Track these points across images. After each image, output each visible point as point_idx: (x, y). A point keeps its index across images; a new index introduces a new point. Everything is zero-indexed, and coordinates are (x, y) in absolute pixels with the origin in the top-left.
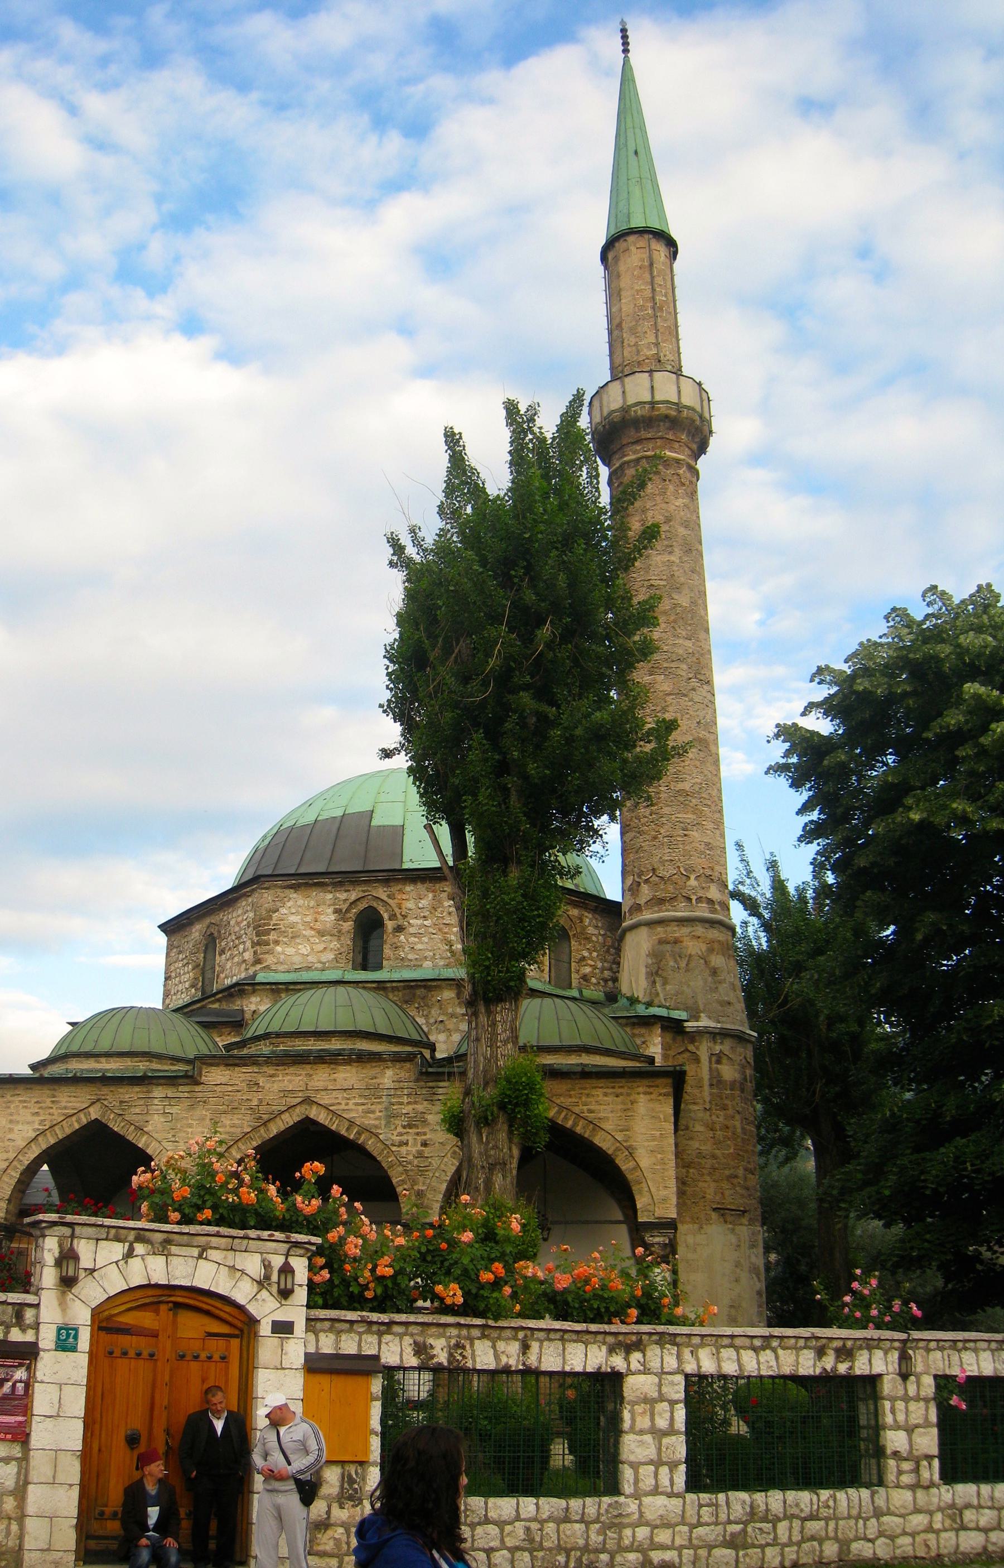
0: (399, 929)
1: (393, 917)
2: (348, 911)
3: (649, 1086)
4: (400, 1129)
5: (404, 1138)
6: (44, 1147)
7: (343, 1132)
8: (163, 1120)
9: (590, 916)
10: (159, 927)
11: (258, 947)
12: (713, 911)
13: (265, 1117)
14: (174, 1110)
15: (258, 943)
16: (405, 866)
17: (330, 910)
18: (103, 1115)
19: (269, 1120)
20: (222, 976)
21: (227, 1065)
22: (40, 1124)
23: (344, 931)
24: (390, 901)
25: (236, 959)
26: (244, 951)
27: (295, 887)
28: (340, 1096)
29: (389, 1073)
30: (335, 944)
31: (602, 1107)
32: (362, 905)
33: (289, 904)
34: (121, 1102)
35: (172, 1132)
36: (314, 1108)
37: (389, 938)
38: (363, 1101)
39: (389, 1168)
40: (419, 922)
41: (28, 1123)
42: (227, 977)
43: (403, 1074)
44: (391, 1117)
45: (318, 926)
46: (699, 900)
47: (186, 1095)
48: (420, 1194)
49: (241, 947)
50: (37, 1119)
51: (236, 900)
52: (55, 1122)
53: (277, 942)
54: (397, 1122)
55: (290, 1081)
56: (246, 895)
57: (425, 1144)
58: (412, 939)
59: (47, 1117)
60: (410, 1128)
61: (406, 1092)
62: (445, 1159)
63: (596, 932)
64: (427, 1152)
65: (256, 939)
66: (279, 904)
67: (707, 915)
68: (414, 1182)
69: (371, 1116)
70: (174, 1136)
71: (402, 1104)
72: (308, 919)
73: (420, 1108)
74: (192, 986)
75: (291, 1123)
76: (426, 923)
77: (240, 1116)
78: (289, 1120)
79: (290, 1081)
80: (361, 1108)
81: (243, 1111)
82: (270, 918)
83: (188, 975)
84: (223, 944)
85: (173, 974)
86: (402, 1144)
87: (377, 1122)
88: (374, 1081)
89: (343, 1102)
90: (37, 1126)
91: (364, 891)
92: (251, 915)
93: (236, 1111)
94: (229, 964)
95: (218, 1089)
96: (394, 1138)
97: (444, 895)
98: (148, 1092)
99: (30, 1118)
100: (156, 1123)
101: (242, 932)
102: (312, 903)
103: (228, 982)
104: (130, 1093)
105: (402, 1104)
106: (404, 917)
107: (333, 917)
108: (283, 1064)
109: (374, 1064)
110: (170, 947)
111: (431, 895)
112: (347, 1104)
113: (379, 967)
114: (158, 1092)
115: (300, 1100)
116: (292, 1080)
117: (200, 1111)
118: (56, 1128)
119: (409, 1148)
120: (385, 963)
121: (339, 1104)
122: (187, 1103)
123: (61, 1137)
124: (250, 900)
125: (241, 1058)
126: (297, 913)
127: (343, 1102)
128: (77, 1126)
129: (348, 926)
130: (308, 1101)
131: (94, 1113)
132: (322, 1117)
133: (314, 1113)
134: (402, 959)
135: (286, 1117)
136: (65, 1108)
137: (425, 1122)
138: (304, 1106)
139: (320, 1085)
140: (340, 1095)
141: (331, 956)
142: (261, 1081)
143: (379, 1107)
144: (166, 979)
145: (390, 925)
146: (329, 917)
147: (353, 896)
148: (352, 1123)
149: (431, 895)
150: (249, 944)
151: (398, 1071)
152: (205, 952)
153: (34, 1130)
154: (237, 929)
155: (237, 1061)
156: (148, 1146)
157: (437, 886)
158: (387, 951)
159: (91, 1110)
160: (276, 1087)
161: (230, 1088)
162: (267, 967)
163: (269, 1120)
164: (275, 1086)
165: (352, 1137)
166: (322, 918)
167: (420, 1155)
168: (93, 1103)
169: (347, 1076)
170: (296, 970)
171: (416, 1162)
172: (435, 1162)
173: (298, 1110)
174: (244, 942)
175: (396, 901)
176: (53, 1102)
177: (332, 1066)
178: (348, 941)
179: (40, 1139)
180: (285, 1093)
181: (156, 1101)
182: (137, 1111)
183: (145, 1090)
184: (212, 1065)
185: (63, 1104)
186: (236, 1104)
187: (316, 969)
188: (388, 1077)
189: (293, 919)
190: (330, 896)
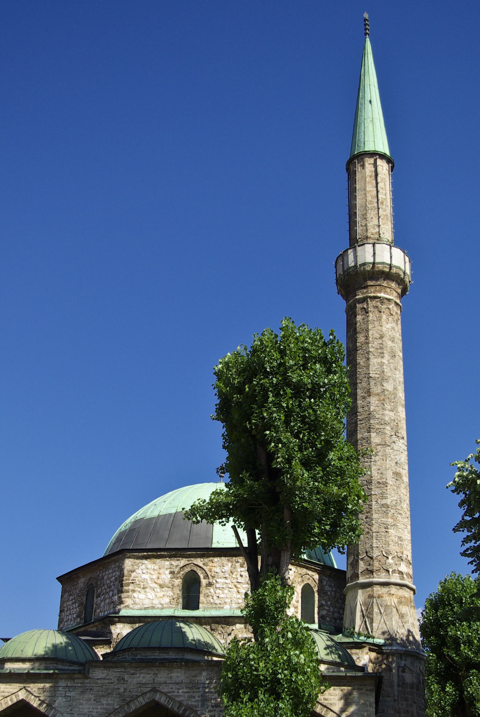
0: (210, 584)
1: (207, 576)
2: (178, 573)
3: (361, 685)
7: (176, 709)
8: (64, 700)
9: (327, 579)
10: (57, 578)
12: (402, 578)
13: (128, 699)
14: (72, 694)
16: (214, 546)
17: (168, 572)
18: (27, 697)
19: (130, 701)
20: (98, 611)
23: (175, 585)
24: (204, 567)
25: (107, 601)
26: (113, 595)
28: (174, 687)
29: (204, 674)
30: (170, 593)
31: (332, 697)
32: (187, 569)
35: (70, 708)
37: (203, 590)
38: (188, 690)
42: (101, 612)
45: (160, 582)
46: (394, 571)
49: (111, 593)
53: (134, 591)
55: (144, 678)
58: (218, 591)
63: (330, 589)
66: (135, 567)
67: (399, 581)
69: (193, 699)
74: (78, 616)
76: (227, 581)
77: (113, 699)
78: (142, 701)
79: (144, 678)
80: (186, 695)
83: (75, 609)
84: (99, 591)
85: (66, 609)
87: (196, 704)
88: (195, 678)
89: (176, 691)
94: (103, 604)
95: (99, 681)
97: (238, 565)
101: (112, 584)
102: (156, 567)
103: (102, 614)
106: (213, 577)
107: (169, 576)
110: (64, 592)
111: (230, 564)
112: (178, 692)
113: (197, 608)
115: (150, 689)
116: (144, 677)
120: (201, 605)
121: (173, 692)
125: (114, 662)
127: (176, 691)
128: (10, 703)
129: (178, 582)
130: (154, 690)
131: (22, 695)
132: (163, 700)
133: (157, 697)
134: (211, 603)
135: (140, 699)
136: (3, 692)
138: (152, 693)
139: (163, 680)
141: (167, 600)
142: (126, 677)
143: (198, 694)
144: (61, 612)
145: (204, 582)
146: (166, 576)
148: (181, 704)
149: (230, 564)
150: (116, 591)
152: (87, 595)
154: (108, 582)
155: (112, 665)
158: (202, 598)
159: (20, 693)
161: (107, 681)
162: (127, 606)
163: (130, 701)
168: (21, 689)
170: (145, 608)
173: (148, 695)
174: (113, 591)
175: (208, 567)
178: (178, 592)
180: (141, 685)
181: (60, 689)
184: (96, 667)
187: (158, 608)
189: (144, 576)
190: (167, 563)
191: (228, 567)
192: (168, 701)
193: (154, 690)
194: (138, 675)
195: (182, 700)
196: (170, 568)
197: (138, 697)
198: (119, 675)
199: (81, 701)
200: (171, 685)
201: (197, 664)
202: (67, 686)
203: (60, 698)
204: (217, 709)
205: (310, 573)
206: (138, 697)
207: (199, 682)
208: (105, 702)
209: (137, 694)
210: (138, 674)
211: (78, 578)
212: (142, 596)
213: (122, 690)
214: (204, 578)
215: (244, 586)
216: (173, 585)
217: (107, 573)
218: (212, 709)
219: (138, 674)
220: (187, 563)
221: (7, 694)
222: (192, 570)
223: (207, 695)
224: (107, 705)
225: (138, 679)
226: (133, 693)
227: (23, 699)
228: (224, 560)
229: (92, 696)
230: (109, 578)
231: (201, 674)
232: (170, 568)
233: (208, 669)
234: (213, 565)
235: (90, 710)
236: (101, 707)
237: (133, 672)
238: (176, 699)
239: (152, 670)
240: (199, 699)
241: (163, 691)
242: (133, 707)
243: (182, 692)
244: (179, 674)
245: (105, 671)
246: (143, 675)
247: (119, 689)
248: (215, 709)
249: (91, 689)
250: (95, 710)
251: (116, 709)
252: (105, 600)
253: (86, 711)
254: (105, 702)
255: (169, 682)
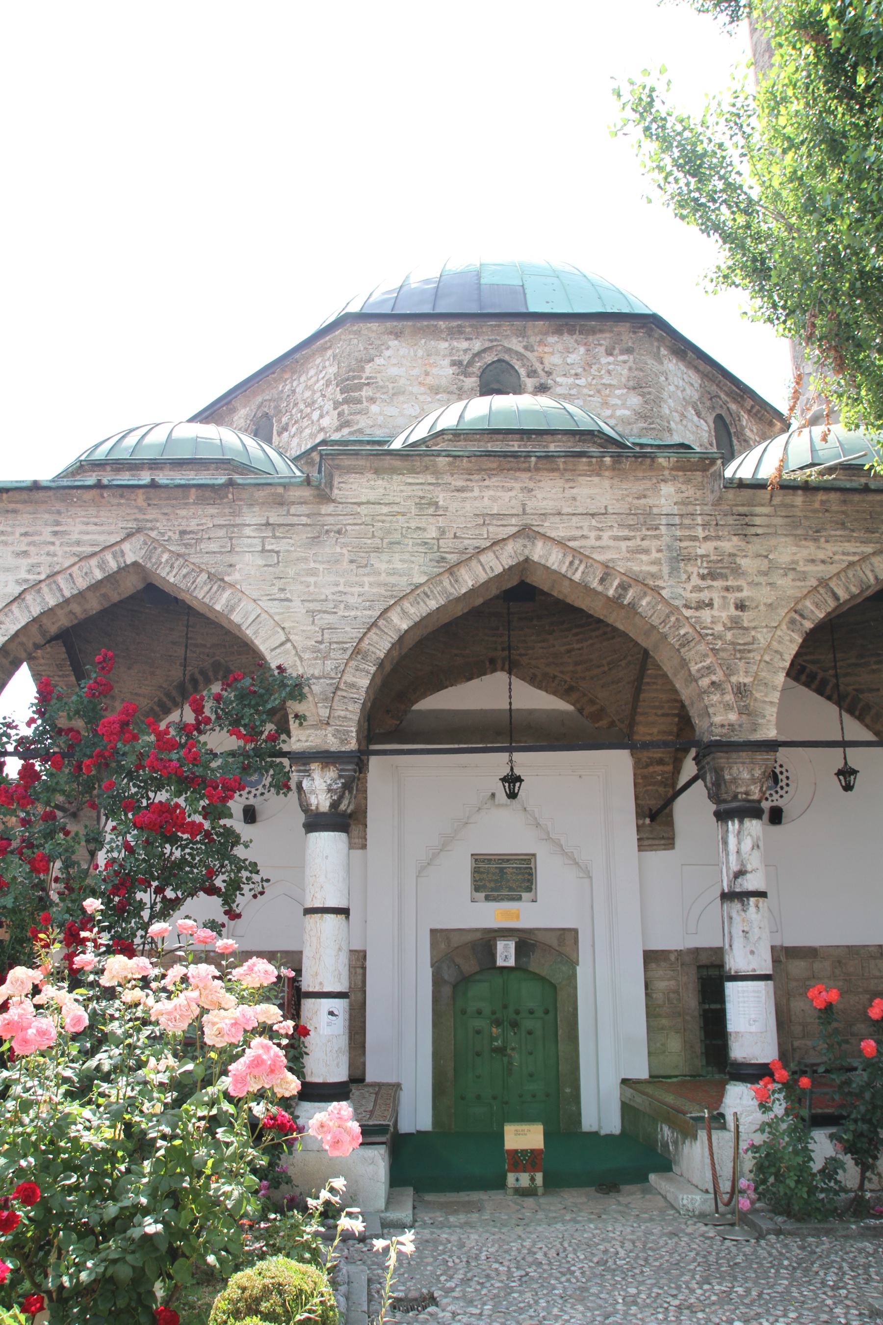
1: (532, 373)
2: (471, 363)
4: (695, 581)
5: (705, 596)
6: (36, 611)
7: (595, 584)
8: (261, 562)
11: (345, 407)
13: (453, 558)
14: (282, 545)
15: (346, 401)
17: (447, 362)
21: (377, 472)
22: (29, 571)
23: (466, 388)
24: (528, 354)
26: (321, 416)
27: (398, 335)
28: (586, 524)
29: (668, 489)
32: (489, 358)
33: (387, 353)
34: (183, 533)
35: (279, 584)
36: (539, 544)
38: (626, 533)
39: (683, 645)
40: (570, 380)
41: (8, 570)
43: (690, 492)
44: (680, 559)
45: (429, 380)
47: (304, 520)
48: (741, 691)
49: (315, 415)
50: (25, 562)
51: (307, 359)
52: (57, 568)
53: (372, 400)
54: (690, 569)
55: (493, 499)
56: (325, 349)
57: (741, 606)
59: (44, 559)
60: (713, 579)
61: (699, 520)
62: (779, 633)
64: (746, 618)
65: (340, 398)
68: (730, 671)
69: (644, 557)
70: (282, 590)
71: (694, 538)
72: (415, 372)
73: (728, 545)
75: (499, 570)
76: (577, 382)
77: (406, 556)
78: (494, 564)
79: (493, 499)
80: (624, 545)
81: (410, 548)
82: (362, 369)
84: (284, 420)
86: (701, 605)
87: (654, 569)
89: (593, 534)
90: (24, 575)
91: (491, 341)
92: (332, 370)
93: (397, 548)
95: (363, 510)
96: (688, 595)
98: (233, 514)
99: (11, 561)
100: (247, 567)
102: (420, 353)
104: (198, 517)
105: (694, 538)
106: (549, 374)
107: (450, 371)
108: (480, 470)
109: (640, 474)
111: (582, 350)
112: (599, 538)
114: (252, 517)
115: (514, 530)
116: (499, 497)
117: (330, 548)
118: (60, 579)
119: (715, 613)
122: (304, 535)
123: (67, 594)
124: (330, 353)
126: (400, 365)
127: (593, 534)
128: (99, 575)
130: (527, 533)
131: (132, 553)
132: (554, 559)
133: (538, 552)
135: (488, 558)
136: (78, 543)
137: (737, 571)
139: (548, 505)
140: (586, 523)
146: (444, 371)
147: (477, 346)
149: (582, 350)
150: (329, 406)
151: (684, 487)
153: (18, 582)
154: (308, 394)
155: (397, 463)
156: (232, 609)
157: (591, 338)
159: (126, 546)
160: (468, 508)
161: (385, 510)
164: (468, 506)
165: (611, 593)
166: (434, 371)
167: (735, 624)
168: (129, 536)
169: (597, 491)
171: (729, 636)
172: (762, 637)
175: (536, 354)
176: (55, 533)
177: (568, 475)
179: (29, 597)
180: (486, 518)
181: (248, 531)
182: (213, 546)
183: (227, 511)
184: (350, 470)
185: (75, 537)
186: (397, 536)
188: (667, 496)
189: (393, 371)
190: (445, 345)
191: (577, 356)
192: (571, 563)
193: (527, 533)
194: (476, 493)
195: (612, 560)
196: (451, 354)
197: (481, 551)
198: (421, 494)
199: (312, 565)
200: (574, 518)
201: (648, 461)
202: (268, 524)
203: (248, 557)
204: (715, 583)
205: (723, 396)
206: (481, 551)
207: (655, 511)
208: (383, 566)
209: (477, 543)
210: (476, 489)
211: (234, 410)
212: (391, 411)
213: (433, 533)
214: (528, 376)
215: (618, 392)
216: (460, 389)
217: (303, 379)
218: (700, 583)
219: (476, 489)
220: (487, 344)
221: (89, 550)
222: (499, 361)
223: (684, 544)
224: (388, 574)
225: (477, 504)
226: (466, 542)
227: (135, 564)
228: (568, 340)
229: (345, 551)
230: (308, 388)
231: (656, 489)
232: (451, 354)
233: (675, 478)
234: (547, 349)
235: (341, 588)
236: (372, 579)
237: (460, 483)
238: (595, 556)
239: (516, 479)
240: (659, 555)
241: (553, 534)
242: (469, 579)
243: (610, 538)
244: (596, 491)
245: (380, 482)
246: (491, 493)
247: (424, 530)
248: (710, 582)
249: (339, 532)
250: (356, 590)
251: (417, 587)
252: (300, 431)
253: (327, 591)
254: (383, 566)
255: (570, 510)
